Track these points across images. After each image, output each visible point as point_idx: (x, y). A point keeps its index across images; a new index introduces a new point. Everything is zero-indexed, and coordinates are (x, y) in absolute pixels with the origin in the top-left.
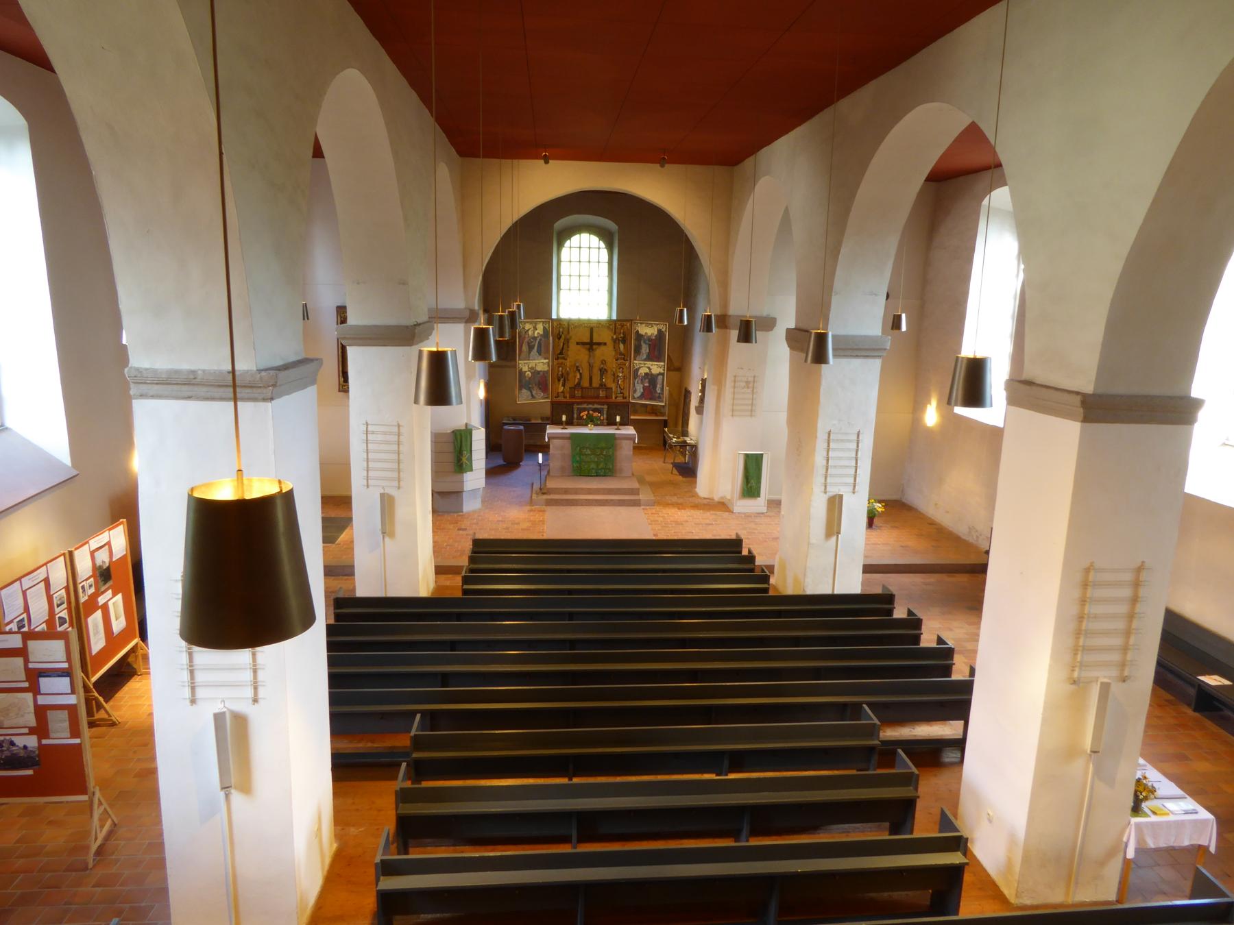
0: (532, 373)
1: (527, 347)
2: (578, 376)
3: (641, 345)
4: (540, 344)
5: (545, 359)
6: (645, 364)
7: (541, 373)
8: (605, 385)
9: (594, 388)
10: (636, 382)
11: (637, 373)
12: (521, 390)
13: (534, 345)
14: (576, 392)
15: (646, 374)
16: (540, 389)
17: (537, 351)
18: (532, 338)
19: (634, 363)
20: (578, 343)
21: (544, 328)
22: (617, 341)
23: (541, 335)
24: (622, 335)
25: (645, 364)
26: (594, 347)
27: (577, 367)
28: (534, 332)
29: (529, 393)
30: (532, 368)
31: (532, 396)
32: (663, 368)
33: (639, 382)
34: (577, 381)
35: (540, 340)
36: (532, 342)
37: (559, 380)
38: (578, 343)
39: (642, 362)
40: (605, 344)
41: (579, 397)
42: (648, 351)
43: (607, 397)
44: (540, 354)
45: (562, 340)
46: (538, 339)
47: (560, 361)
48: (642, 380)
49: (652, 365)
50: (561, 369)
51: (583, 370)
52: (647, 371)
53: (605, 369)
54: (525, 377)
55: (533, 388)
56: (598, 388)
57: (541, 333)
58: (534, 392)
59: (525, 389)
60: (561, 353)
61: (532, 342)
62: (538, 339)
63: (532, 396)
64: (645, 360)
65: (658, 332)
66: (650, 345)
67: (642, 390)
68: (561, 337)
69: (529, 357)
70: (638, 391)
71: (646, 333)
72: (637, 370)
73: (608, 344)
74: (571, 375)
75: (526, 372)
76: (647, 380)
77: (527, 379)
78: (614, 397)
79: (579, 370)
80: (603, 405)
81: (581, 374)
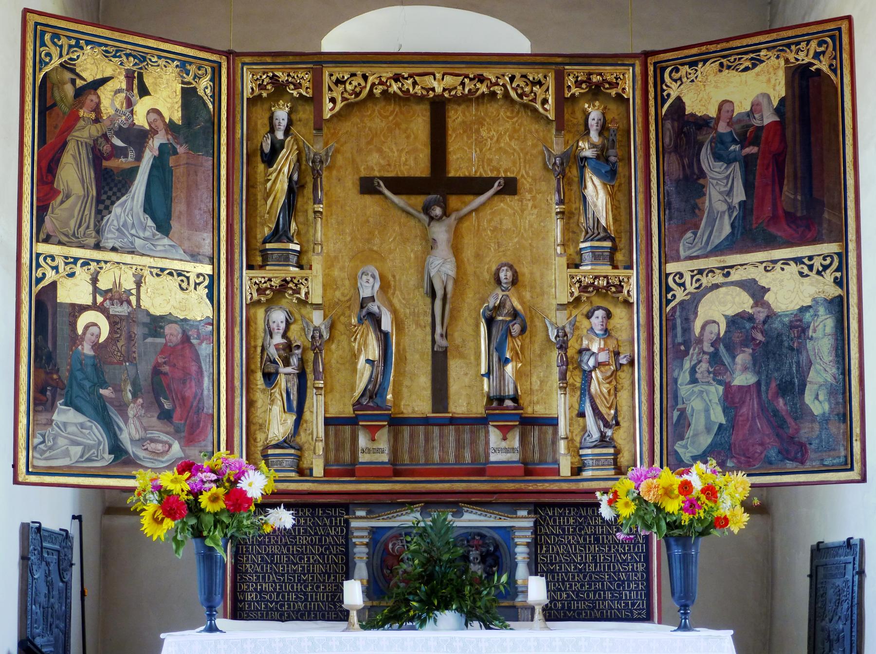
0: (114, 321)
1: (89, 174)
2: (373, 350)
3: (702, 174)
4: (160, 166)
5: (195, 257)
6: (726, 271)
7: (169, 329)
8: (515, 399)
9: (454, 421)
10: (684, 377)
11: (687, 330)
12: (51, 408)
13: (133, 172)
14: (363, 441)
15: (734, 321)
16: (165, 416)
17: (148, 208)
18: (121, 133)
19: (664, 276)
20: (368, 186)
21: (189, 95)
22: (574, 172)
23: (171, 127)
24: (594, 136)
25: (726, 271)
26: (454, 201)
27: (363, 303)
28: (130, 104)
29: (96, 433)
30: (116, 295)
31: (117, 449)
32: (829, 276)
33: (704, 366)
34: (364, 373)
35: (164, 151)
36: (117, 152)
37: (270, 378)
38: (368, 186)
39: (712, 262)
40: (510, 187)
41: (375, 472)
42: (739, 195)
43: (528, 469)
44: (163, 227)
45: (285, 164)
46: (156, 142)
47: (275, 274)
48: (715, 358)
49: (769, 266)
50: (278, 317)
51: (398, 323)
52: (743, 302)
53: (515, 314)
54: (75, 339)
55: (122, 409)
56: (483, 421)
57: (173, 111)
58: (128, 433)
59: (69, 403)
60: (279, 234)
61: (117, 152)
62: (156, 142)
63: (117, 449)
64: (731, 245)
65: (789, 84)
66: (748, 164)
67: (718, 416)
68: (276, 148)
69: (98, 231)
70: (698, 423)
71: (725, 105)
72: (690, 306)
73: (525, 183)
74: (335, 353)
75: (78, 309)
76: (743, 358)
77: (87, 349)
78: (565, 471)
79: (376, 320)
80: (513, 514)
81: (384, 339)
